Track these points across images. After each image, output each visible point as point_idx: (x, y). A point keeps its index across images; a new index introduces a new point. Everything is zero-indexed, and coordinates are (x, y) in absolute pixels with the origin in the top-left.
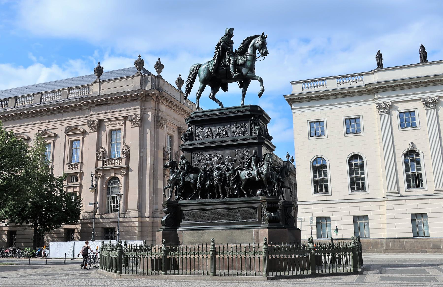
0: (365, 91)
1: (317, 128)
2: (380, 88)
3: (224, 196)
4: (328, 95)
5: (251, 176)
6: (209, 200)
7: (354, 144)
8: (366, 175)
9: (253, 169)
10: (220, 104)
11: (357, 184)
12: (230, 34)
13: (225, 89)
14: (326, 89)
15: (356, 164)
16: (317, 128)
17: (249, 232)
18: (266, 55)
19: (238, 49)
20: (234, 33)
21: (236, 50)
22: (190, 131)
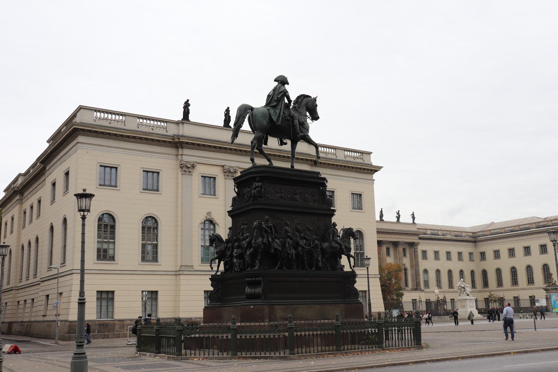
0: (170, 142)
1: (109, 175)
2: (187, 143)
4: (128, 137)
7: (151, 205)
8: (141, 242)
11: (150, 253)
15: (150, 227)
16: (109, 175)
18: (316, 120)
22: (261, 186)
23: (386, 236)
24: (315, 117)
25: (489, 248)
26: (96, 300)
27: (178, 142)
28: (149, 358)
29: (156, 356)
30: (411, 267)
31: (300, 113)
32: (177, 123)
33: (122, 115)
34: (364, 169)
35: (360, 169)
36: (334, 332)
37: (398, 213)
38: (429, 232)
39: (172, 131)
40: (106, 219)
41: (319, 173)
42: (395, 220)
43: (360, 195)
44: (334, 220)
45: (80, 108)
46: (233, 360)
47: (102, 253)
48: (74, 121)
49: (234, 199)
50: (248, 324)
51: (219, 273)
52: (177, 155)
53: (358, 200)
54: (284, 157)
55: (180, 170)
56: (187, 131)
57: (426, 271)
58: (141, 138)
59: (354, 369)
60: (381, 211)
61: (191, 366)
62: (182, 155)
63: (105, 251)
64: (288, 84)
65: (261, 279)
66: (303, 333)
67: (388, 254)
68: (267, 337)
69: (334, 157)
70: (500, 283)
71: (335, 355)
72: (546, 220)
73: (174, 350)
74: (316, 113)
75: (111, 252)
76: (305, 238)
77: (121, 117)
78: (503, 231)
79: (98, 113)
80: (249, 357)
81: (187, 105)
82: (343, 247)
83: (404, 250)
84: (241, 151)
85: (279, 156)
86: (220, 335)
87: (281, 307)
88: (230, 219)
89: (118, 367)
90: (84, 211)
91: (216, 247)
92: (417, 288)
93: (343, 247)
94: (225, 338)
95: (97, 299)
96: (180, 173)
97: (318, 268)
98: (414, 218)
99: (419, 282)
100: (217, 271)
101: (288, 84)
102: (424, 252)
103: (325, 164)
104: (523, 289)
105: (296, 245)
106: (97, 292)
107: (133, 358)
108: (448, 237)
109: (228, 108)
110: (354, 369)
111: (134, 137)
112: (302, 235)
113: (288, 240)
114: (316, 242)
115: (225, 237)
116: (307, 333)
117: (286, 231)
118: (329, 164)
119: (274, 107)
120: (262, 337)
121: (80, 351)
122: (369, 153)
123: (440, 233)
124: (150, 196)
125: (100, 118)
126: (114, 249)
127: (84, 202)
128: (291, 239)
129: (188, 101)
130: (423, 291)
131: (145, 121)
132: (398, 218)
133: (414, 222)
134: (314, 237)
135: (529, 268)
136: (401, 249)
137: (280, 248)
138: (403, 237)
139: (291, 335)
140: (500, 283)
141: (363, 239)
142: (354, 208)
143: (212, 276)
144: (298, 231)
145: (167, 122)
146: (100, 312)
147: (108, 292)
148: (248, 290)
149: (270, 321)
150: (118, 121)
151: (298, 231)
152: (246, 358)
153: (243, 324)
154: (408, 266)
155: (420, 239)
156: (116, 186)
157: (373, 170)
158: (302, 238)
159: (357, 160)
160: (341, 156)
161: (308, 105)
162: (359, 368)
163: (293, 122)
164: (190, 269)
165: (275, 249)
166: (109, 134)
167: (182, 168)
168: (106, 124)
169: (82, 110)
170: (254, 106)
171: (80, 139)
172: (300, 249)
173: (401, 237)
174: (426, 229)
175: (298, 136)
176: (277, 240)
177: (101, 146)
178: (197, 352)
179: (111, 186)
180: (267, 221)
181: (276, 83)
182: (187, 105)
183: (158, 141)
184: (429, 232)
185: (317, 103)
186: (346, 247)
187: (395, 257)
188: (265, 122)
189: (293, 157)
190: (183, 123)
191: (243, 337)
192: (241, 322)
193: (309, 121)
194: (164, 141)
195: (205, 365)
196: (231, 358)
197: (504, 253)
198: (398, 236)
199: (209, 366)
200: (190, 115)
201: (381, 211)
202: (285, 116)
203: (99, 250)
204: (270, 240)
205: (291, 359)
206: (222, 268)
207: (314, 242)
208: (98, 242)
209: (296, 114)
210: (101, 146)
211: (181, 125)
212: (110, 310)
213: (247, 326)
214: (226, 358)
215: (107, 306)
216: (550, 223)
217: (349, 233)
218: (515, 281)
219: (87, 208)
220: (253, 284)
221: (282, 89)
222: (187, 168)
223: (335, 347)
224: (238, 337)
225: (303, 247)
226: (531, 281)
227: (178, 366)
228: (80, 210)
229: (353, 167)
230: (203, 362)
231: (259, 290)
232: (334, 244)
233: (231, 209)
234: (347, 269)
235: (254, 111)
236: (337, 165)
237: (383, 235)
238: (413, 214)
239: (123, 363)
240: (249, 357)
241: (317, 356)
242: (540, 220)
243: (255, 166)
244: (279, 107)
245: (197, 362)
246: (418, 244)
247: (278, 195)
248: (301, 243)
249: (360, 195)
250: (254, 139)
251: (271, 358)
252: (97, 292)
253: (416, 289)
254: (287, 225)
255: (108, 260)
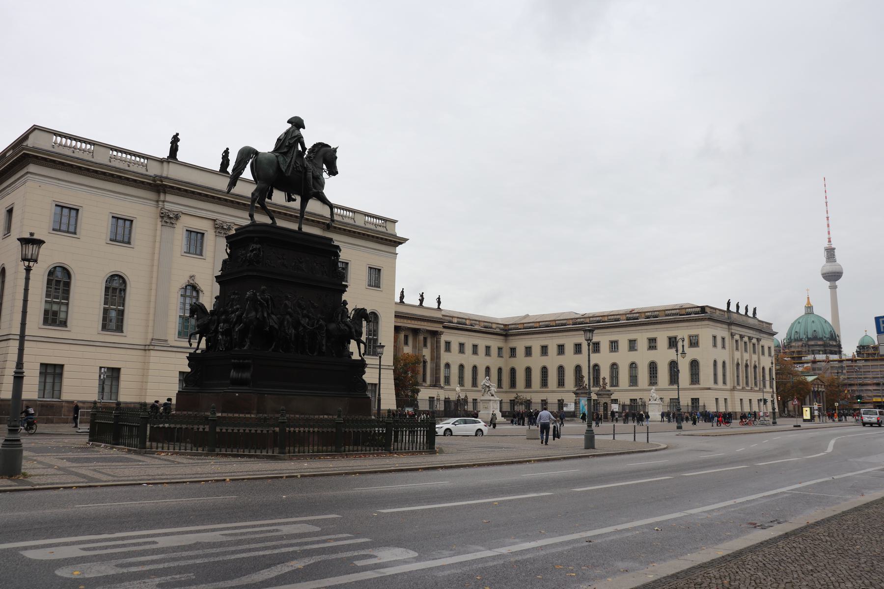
0: (150, 184)
1: (67, 218)
2: (172, 187)
4: (96, 172)
7: (119, 260)
8: (103, 306)
11: (113, 320)
14: (91, 159)
15: (116, 288)
16: (67, 218)
23: (405, 321)
24: (333, 172)
25: (520, 344)
26: (38, 374)
27: (161, 185)
28: (103, 450)
29: (112, 448)
30: (432, 359)
31: (315, 165)
32: (161, 161)
33: (89, 143)
34: (386, 240)
35: (382, 239)
36: (334, 430)
37: (422, 296)
38: (455, 320)
39: (154, 170)
40: (59, 274)
41: (331, 240)
42: (418, 303)
43: (379, 270)
44: (344, 297)
45: (35, 128)
46: (209, 457)
47: (50, 316)
48: (25, 144)
49: (225, 262)
50: (230, 415)
51: (199, 351)
52: (157, 201)
53: (376, 277)
54: (291, 215)
55: (160, 219)
56: (173, 172)
57: (448, 366)
58: (112, 175)
59: (355, 473)
60: (402, 292)
61: (157, 462)
62: (164, 201)
63: (55, 313)
64: (304, 128)
65: (250, 361)
66: (297, 429)
67: (406, 343)
68: (253, 431)
69: (352, 222)
70: (528, 384)
71: (333, 456)
72: (584, 317)
73: (136, 441)
74: (335, 167)
75: (62, 316)
76: (308, 317)
77: (88, 146)
78: (537, 325)
79: (59, 138)
80: (230, 455)
81: (175, 140)
82: (353, 330)
83: (425, 339)
84: (238, 203)
85: (285, 214)
86: (196, 427)
88: (217, 287)
89: (62, 459)
90: (29, 260)
91: (197, 319)
92: (436, 384)
93: (353, 330)
94: (201, 430)
95: (41, 373)
96: (159, 224)
98: (439, 303)
99: (439, 377)
100: (197, 348)
101: (304, 128)
102: (448, 344)
103: (340, 229)
104: (553, 392)
105: (297, 324)
106: (42, 364)
107: (83, 449)
108: (477, 327)
109: (228, 149)
110: (355, 473)
111: (104, 174)
112: (305, 312)
113: (288, 317)
114: (321, 322)
115: (209, 306)
116: (302, 429)
118: (345, 230)
119: (285, 154)
120: (247, 431)
121: (13, 437)
122: (394, 222)
123: (468, 322)
124: (119, 250)
125: (60, 145)
126: (67, 312)
127: (30, 250)
128: (291, 316)
129: (177, 134)
130: (442, 388)
131: (120, 154)
132: (422, 301)
133: (439, 308)
134: (319, 315)
135: (561, 369)
136: (421, 338)
137: (276, 326)
138: (426, 324)
140: (528, 384)
141: (377, 323)
142: (370, 285)
143: (190, 354)
145: (147, 159)
146: (43, 390)
147: (55, 366)
148: (233, 374)
149: (258, 413)
150: (84, 151)
152: (226, 455)
153: (225, 415)
154: (428, 358)
155: (444, 327)
156: (75, 233)
157: (397, 242)
158: (304, 316)
159: (379, 229)
160: (360, 221)
161: (326, 156)
162: (360, 473)
164: (163, 343)
165: (271, 327)
166: (72, 166)
167: (162, 217)
168: (69, 152)
169: (36, 131)
170: (260, 149)
171: (32, 168)
172: (301, 329)
173: (423, 323)
174: (452, 317)
176: (273, 316)
177: (59, 180)
178: (166, 445)
179: (68, 232)
180: (263, 292)
181: (290, 125)
182: (175, 140)
183: (135, 181)
184: (455, 320)
185: (337, 154)
186: (356, 331)
187: (414, 347)
188: (271, 171)
189: (301, 216)
190: (169, 162)
191: (224, 431)
192: (222, 412)
193: (325, 175)
194: (143, 182)
195: (173, 462)
196: (207, 455)
197: (536, 351)
198: (419, 323)
199: (179, 463)
200: (178, 153)
201: (402, 292)
202: (297, 165)
203: (46, 312)
204: (265, 315)
205: (281, 459)
206: (203, 345)
207: (318, 321)
208: (46, 302)
209: (310, 166)
210: (59, 180)
211: (165, 164)
212: (57, 388)
213: (230, 418)
214: (201, 455)
215: (54, 383)
216: (588, 320)
217: (361, 314)
218: (544, 383)
219: (34, 257)
220: (240, 367)
221: (296, 133)
222: (169, 219)
223: (334, 448)
224: (218, 430)
225: (304, 327)
226: (561, 383)
227: (140, 461)
228: (24, 259)
229: (373, 236)
230: (171, 458)
231: (247, 375)
232: (342, 326)
233: (219, 274)
234: (356, 356)
235: (260, 156)
236: (354, 232)
237: (402, 320)
238: (439, 298)
239: (70, 455)
240: (230, 455)
241: (311, 457)
242: (577, 316)
243: (254, 224)
244: (290, 155)
245: (165, 457)
246: (441, 333)
248: (302, 322)
249: (379, 270)
250: (256, 190)
251: (257, 457)
252: (42, 364)
253: (435, 386)
255: (58, 326)
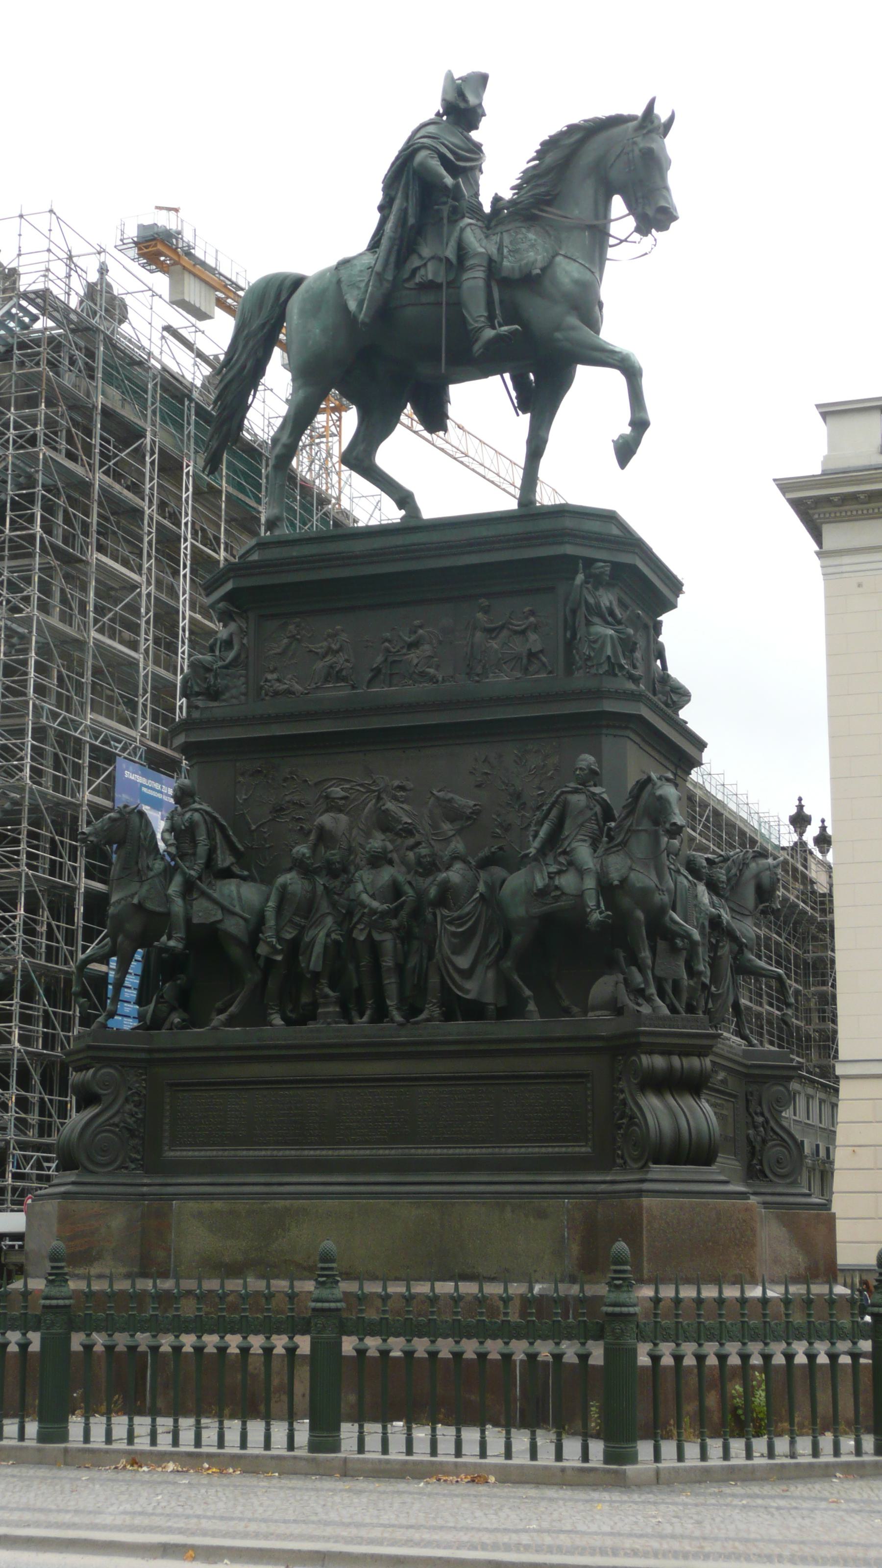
3: (412, 1011)
5: (557, 899)
6: (327, 1028)
9: (571, 863)
10: (404, 499)
12: (462, 108)
13: (434, 418)
17: (541, 1214)
18: (663, 226)
19: (507, 195)
20: (490, 100)
21: (497, 200)
24: (654, 215)
87: (204, 1206)
93: (590, 883)
97: (456, 1008)
114: (455, 875)
116: (257, 1342)
117: (324, 837)
139: (56, 1345)
144: (385, 823)
151: (385, 823)
163: (454, 284)
175: (477, 347)
247: (320, 665)
254: (332, 805)
